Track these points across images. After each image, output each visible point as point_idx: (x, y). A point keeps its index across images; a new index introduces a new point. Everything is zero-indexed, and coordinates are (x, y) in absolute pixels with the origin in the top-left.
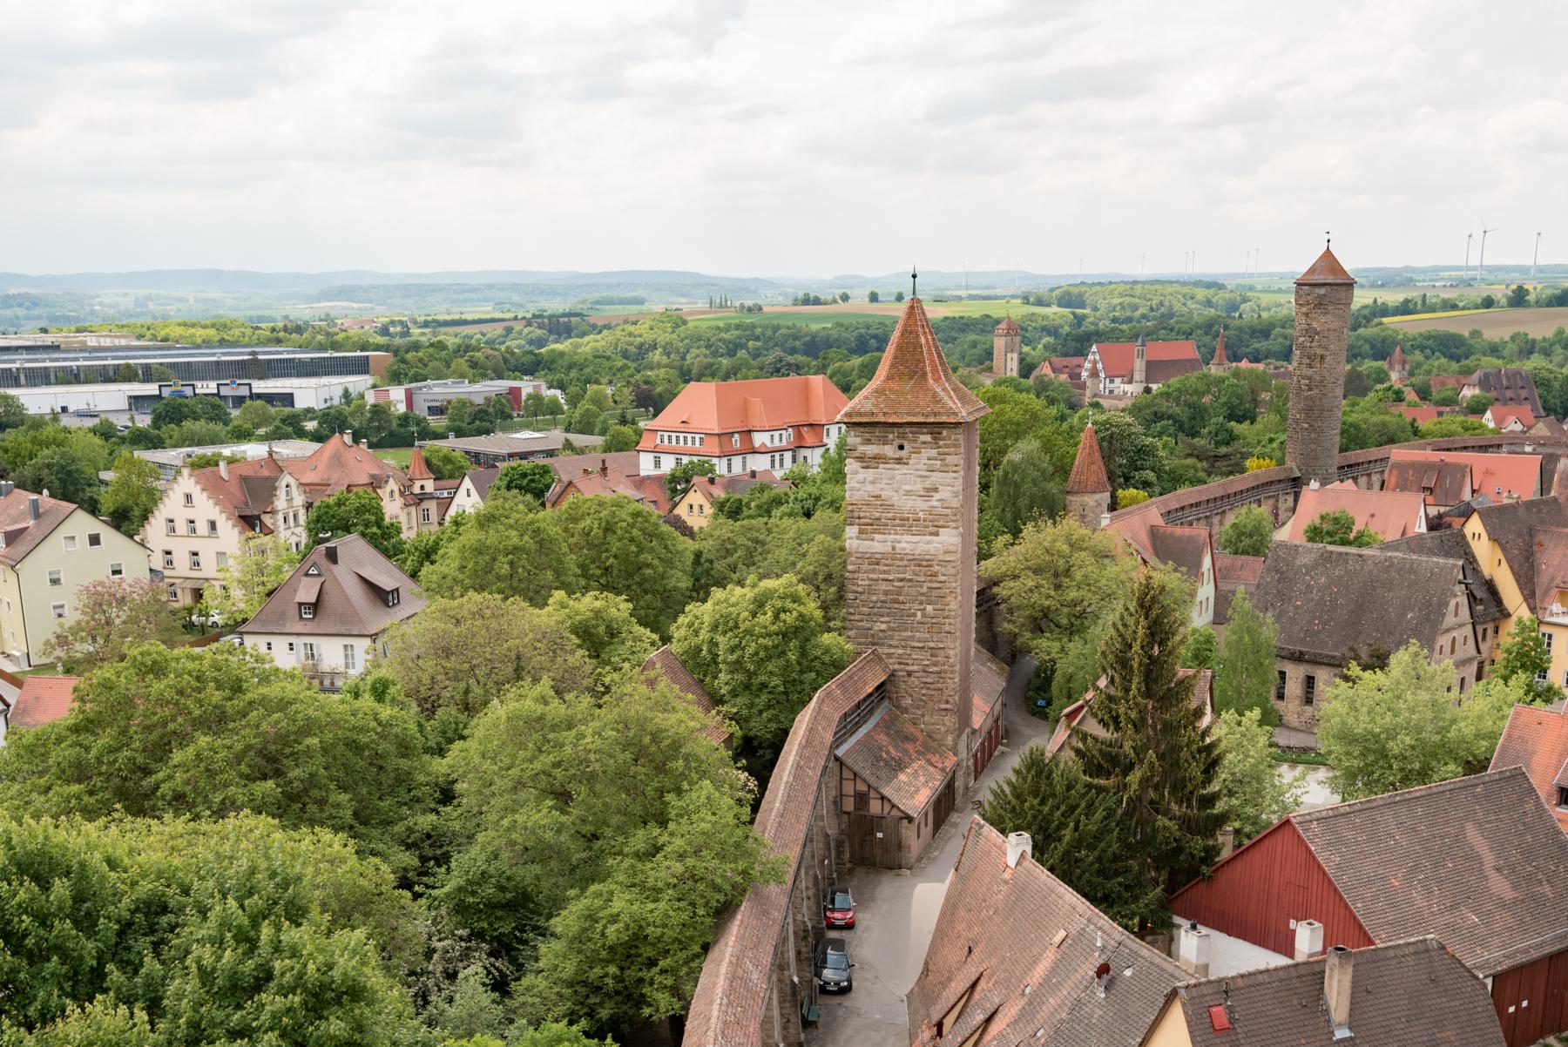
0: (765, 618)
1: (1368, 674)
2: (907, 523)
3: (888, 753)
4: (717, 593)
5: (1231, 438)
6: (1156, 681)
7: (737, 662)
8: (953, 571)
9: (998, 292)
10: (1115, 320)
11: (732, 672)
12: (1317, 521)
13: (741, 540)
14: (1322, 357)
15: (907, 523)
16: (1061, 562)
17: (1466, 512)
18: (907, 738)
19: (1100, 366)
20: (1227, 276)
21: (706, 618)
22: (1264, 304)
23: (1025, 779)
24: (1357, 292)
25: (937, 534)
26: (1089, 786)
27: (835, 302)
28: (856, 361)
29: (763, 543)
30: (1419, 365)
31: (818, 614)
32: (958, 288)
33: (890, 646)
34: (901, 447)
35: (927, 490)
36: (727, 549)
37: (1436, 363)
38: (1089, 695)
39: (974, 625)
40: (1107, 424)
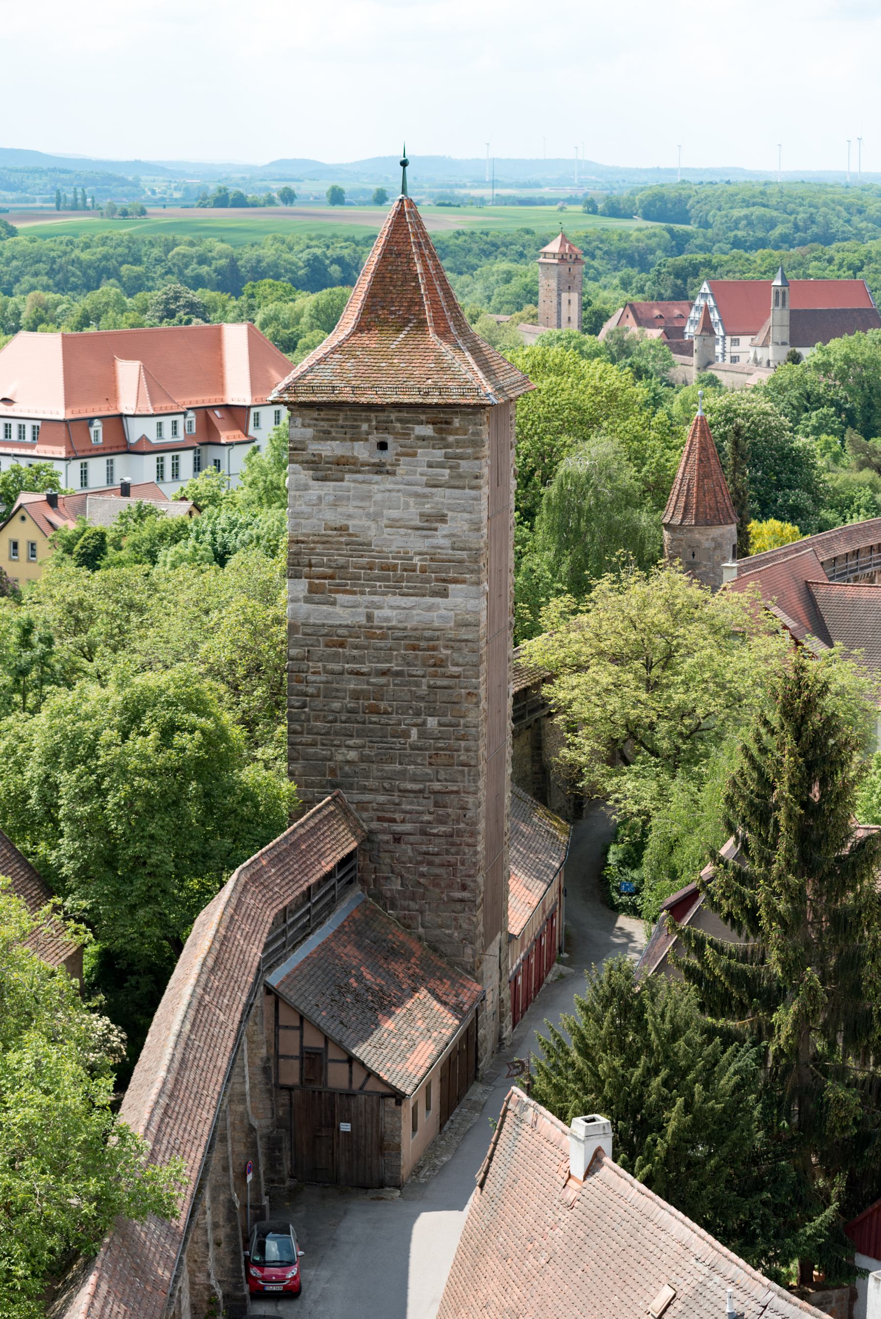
0: (144, 744)
2: (394, 575)
3: (360, 978)
4: (60, 698)
6: (817, 845)
7: (91, 817)
9: (546, 192)
10: (737, 244)
11: (82, 836)
13: (101, 605)
15: (394, 575)
18: (394, 953)
19: (715, 316)
21: (38, 740)
23: (599, 1020)
25: (444, 594)
26: (710, 1032)
27: (270, 201)
28: (306, 301)
29: (141, 611)
31: (237, 733)
32: (479, 183)
33: (364, 789)
34: (383, 446)
35: (426, 517)
36: (77, 617)
39: (509, 752)
40: (728, 414)
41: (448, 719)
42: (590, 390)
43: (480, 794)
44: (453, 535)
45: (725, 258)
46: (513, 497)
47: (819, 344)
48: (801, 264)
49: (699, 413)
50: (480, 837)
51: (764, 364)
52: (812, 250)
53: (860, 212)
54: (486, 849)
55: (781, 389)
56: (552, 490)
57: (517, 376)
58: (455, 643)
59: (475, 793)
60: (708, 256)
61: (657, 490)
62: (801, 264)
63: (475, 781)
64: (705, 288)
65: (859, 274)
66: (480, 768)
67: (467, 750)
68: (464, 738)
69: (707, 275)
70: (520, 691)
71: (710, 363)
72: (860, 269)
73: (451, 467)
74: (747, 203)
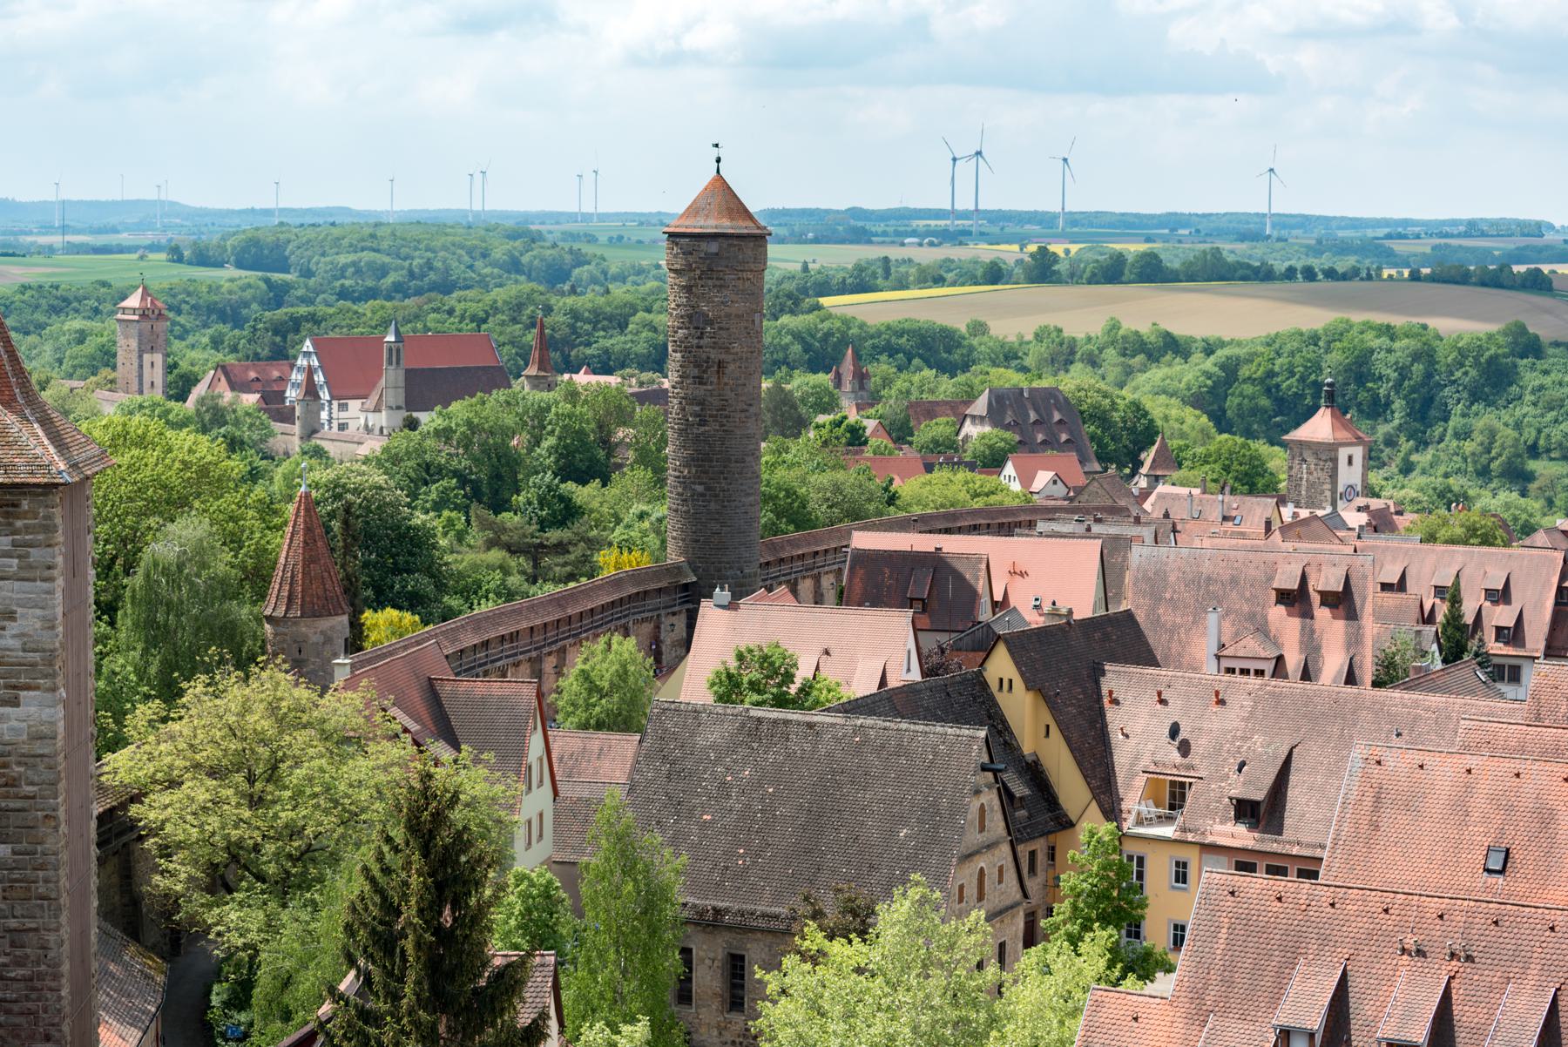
1: (837, 948)
5: (568, 512)
6: (451, 976)
8: (48, 776)
10: (343, 294)
12: (733, 665)
14: (720, 365)
16: (263, 751)
17: (986, 643)
19: (319, 378)
20: (544, 217)
22: (613, 270)
24: (773, 250)
25: (15, 702)
30: (887, 382)
37: (916, 378)
38: (326, 1009)
39: (94, 882)
40: (336, 489)
41: (24, 846)
42: (177, 465)
43: (62, 931)
44: (22, 635)
45: (331, 311)
46: (91, 590)
47: (438, 408)
48: (417, 317)
49: (303, 489)
50: (64, 981)
51: (377, 431)
52: (430, 301)
53: (484, 256)
54: (71, 993)
55: (396, 460)
56: (137, 580)
57: (96, 451)
58: (29, 759)
59: (57, 930)
60: (311, 309)
61: (257, 577)
62: (417, 317)
63: (56, 917)
64: (308, 345)
65: (484, 327)
66: (62, 901)
67: (46, 881)
68: (42, 867)
69: (309, 330)
70: (105, 812)
71: (315, 431)
72: (485, 321)
73: (19, 557)
74: (353, 248)
